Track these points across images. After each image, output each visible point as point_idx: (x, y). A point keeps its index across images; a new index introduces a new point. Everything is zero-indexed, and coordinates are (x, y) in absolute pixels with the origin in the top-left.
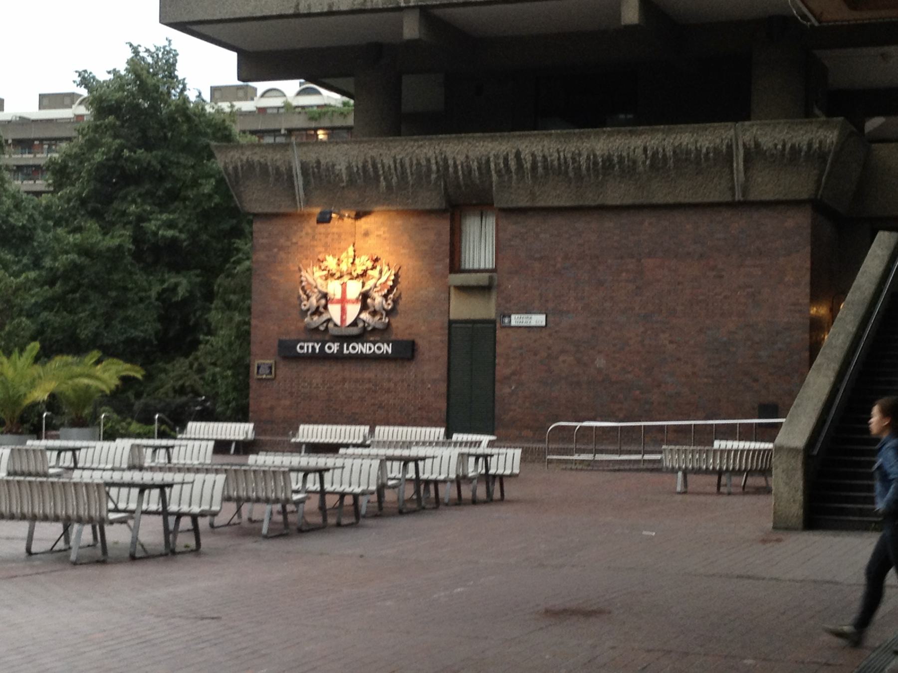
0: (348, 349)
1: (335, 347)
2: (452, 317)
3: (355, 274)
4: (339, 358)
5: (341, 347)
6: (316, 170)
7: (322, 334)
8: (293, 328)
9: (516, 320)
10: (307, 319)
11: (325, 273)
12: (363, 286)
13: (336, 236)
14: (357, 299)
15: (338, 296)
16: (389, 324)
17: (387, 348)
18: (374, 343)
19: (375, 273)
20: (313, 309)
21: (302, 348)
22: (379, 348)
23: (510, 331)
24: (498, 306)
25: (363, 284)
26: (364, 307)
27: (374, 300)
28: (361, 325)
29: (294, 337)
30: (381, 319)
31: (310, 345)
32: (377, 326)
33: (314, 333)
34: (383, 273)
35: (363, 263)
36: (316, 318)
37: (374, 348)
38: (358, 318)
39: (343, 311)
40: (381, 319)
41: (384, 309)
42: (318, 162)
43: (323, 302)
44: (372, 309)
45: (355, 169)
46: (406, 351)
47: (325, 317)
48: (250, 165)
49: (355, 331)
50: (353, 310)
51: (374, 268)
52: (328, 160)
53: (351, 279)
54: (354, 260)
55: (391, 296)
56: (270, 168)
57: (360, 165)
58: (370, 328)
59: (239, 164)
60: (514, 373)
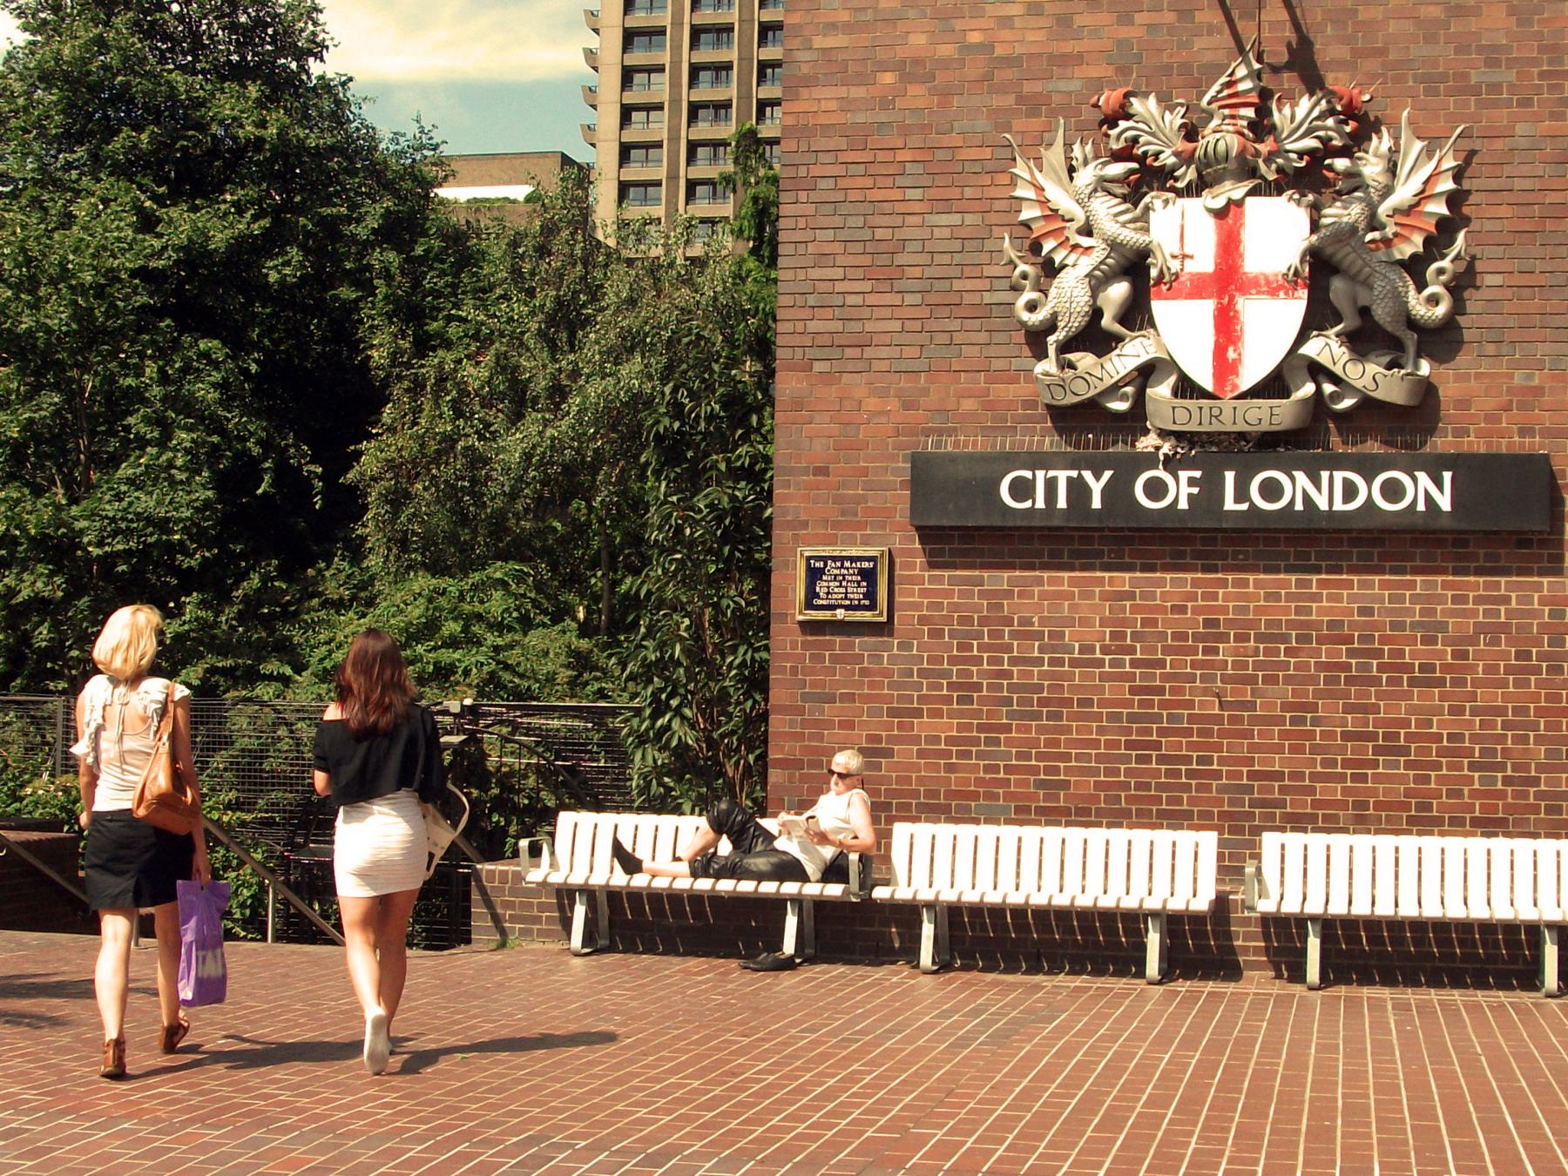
0: (1242, 494)
5: (1210, 489)
8: (968, 405)
11: (1118, 169)
12: (1315, 227)
14: (1291, 281)
15: (1204, 261)
20: (1077, 322)
21: (1022, 489)
29: (976, 443)
31: (1062, 476)
32: (1379, 395)
33: (1087, 424)
34: (1403, 172)
37: (1369, 491)
39: (1227, 327)
41: (1412, 323)
43: (1119, 291)
50: (1271, 328)
51: (1355, 144)
53: (1253, 192)
54: (1263, 111)
55: (1445, 263)
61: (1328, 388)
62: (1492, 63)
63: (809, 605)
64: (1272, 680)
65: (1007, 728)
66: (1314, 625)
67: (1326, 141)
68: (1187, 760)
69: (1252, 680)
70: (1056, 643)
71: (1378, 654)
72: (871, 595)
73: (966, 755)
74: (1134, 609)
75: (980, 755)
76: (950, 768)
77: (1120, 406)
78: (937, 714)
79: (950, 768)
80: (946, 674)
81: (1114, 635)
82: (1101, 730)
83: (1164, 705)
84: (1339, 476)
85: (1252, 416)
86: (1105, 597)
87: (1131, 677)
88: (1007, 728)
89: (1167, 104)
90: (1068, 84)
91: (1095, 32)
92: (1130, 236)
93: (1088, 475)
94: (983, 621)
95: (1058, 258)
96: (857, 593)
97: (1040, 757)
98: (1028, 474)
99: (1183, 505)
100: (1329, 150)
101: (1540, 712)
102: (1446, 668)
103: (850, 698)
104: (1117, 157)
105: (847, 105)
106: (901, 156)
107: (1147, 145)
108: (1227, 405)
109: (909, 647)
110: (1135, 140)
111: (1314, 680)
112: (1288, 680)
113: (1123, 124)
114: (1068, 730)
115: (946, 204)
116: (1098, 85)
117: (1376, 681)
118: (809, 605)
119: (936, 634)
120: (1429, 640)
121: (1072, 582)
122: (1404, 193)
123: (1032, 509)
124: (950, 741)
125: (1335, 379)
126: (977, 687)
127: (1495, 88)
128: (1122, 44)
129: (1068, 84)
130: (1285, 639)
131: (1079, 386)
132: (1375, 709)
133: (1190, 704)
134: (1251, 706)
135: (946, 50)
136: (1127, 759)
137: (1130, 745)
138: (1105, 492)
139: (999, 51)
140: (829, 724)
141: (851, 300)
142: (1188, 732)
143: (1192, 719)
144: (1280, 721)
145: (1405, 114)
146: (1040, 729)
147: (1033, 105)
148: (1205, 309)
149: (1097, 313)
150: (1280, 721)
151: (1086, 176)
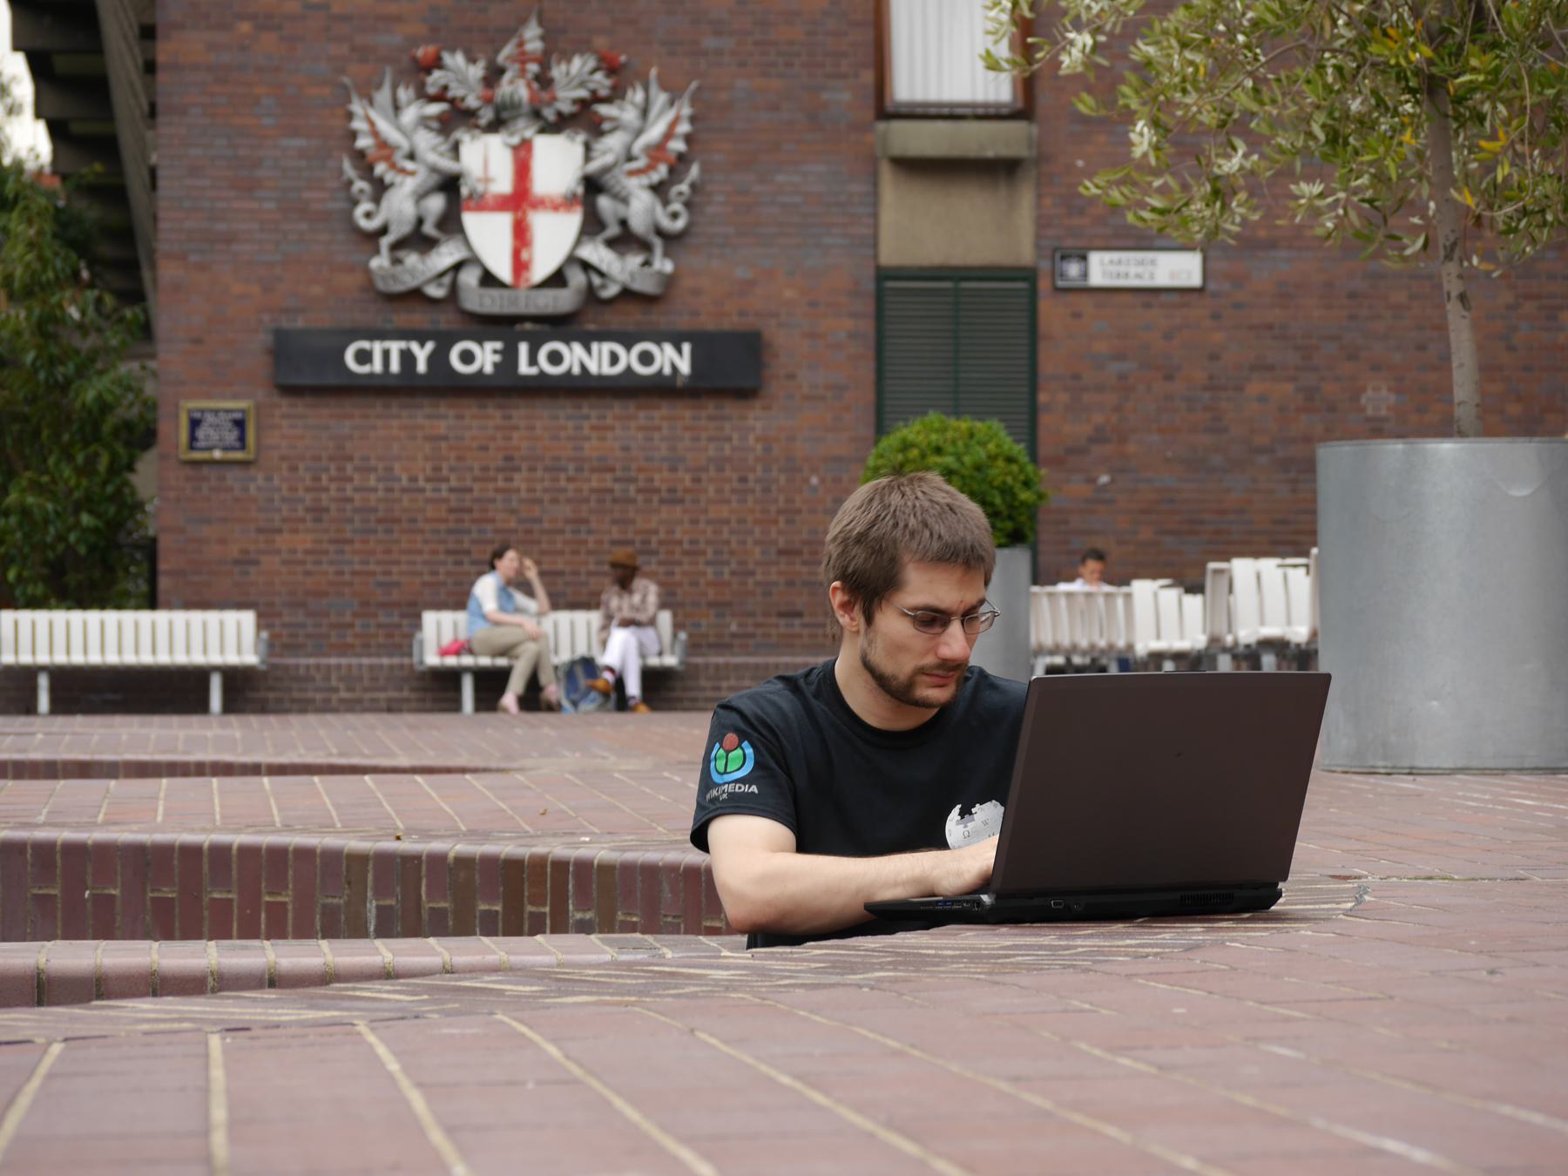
0: (533, 361)
1: (486, 357)
2: (890, 255)
3: (549, 114)
4: (506, 388)
5: (509, 356)
7: (445, 314)
8: (317, 290)
9: (1103, 268)
10: (380, 262)
11: (435, 109)
12: (588, 158)
14: (568, 202)
15: (503, 184)
16: (669, 281)
17: (673, 359)
18: (628, 342)
19: (627, 113)
21: (364, 357)
22: (646, 358)
23: (1085, 303)
24: (1042, 223)
25: (588, 148)
26: (592, 225)
27: (625, 201)
28: (577, 278)
30: (647, 263)
31: (395, 347)
35: (575, 75)
36: (411, 259)
37: (629, 359)
38: (572, 259)
39: (521, 234)
40: (647, 263)
41: (659, 232)
43: (436, 203)
44: (613, 230)
46: (733, 368)
47: (446, 256)
49: (561, 301)
50: (555, 238)
51: (616, 94)
53: (542, 131)
55: (684, 187)
58: (611, 291)
60: (1099, 437)
61: (597, 280)
62: (718, 33)
63: (192, 447)
64: (555, 501)
65: (351, 541)
69: (540, 501)
71: (634, 480)
72: (242, 438)
73: (318, 563)
74: (450, 448)
76: (308, 573)
77: (435, 291)
78: (295, 531)
79: (308, 573)
80: (302, 500)
81: (437, 469)
82: (426, 542)
87: (446, 500)
88: (351, 541)
89: (472, 60)
90: (392, 39)
92: (447, 164)
93: (414, 346)
95: (388, 178)
96: (231, 436)
99: (489, 369)
100: (596, 99)
101: (756, 522)
102: (686, 491)
104: (434, 99)
107: (455, 91)
108: (522, 293)
109: (269, 479)
110: (445, 88)
111: (587, 501)
112: (569, 501)
113: (437, 74)
114: (398, 542)
115: (295, 132)
116: (415, 42)
117: (633, 501)
118: (192, 447)
119: (294, 469)
120: (673, 469)
122: (655, 132)
123: (371, 375)
124: (307, 552)
125: (602, 274)
126: (327, 510)
127: (719, 52)
129: (392, 39)
132: (633, 522)
134: (539, 521)
137: (448, 552)
138: (431, 360)
139: (335, 10)
145: (653, 72)
149: (420, 221)
151: (410, 115)
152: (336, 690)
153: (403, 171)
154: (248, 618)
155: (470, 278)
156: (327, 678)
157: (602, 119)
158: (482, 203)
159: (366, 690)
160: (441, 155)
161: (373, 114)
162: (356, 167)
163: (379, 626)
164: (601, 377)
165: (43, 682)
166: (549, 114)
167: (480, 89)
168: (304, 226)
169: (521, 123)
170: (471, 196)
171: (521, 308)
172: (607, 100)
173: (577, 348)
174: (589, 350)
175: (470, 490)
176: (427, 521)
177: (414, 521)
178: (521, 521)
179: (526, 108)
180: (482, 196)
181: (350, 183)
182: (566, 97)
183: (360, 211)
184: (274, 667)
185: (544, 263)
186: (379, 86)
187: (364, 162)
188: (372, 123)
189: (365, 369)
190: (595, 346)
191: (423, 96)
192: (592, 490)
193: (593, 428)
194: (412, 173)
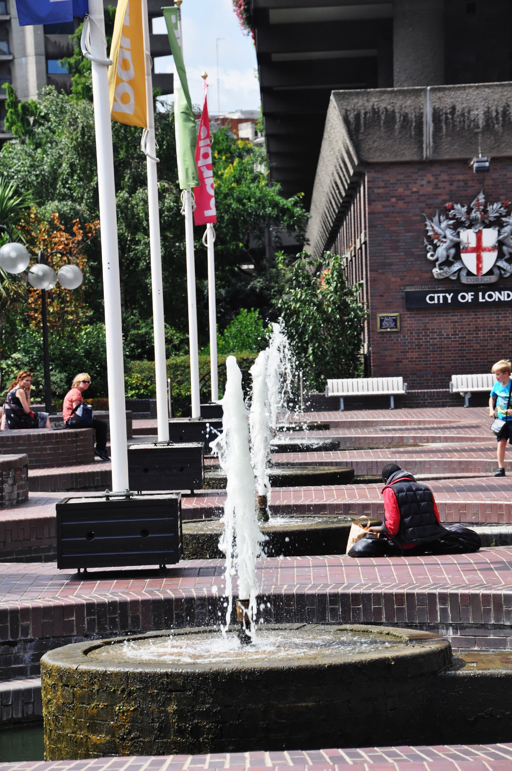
0: (483, 298)
1: (469, 297)
5: (476, 297)
6: (450, 116)
8: (417, 279)
10: (436, 271)
11: (451, 222)
12: (499, 235)
13: (462, 184)
15: (473, 244)
20: (444, 259)
21: (432, 299)
25: (499, 231)
28: (496, 271)
31: (441, 295)
36: (446, 268)
38: (495, 266)
39: (479, 260)
42: (454, 108)
43: (452, 251)
45: (494, 114)
48: (375, 112)
49: (493, 279)
50: (489, 259)
52: (464, 105)
53: (484, 228)
54: (486, 206)
56: (398, 115)
57: (500, 109)
59: (363, 112)
61: (503, 272)
63: (381, 328)
64: (491, 340)
65: (429, 354)
66: (501, 327)
67: (501, 214)
68: (472, 359)
69: (487, 340)
70: (440, 334)
72: (396, 325)
73: (420, 361)
75: (423, 361)
77: (454, 278)
78: (413, 352)
79: (416, 364)
80: (414, 343)
81: (454, 331)
82: (452, 354)
83: (467, 347)
84: (506, 292)
85: (486, 280)
86: (452, 322)
87: (458, 341)
88: (429, 354)
89: (463, 206)
90: (439, 200)
91: (444, 188)
92: (456, 239)
93: (447, 295)
94: (423, 330)
95: (438, 244)
96: (392, 325)
97: (438, 360)
98: (433, 295)
99: (470, 301)
100: (501, 216)
103: (392, 349)
105: (384, 207)
106: (398, 219)
107: (458, 216)
108: (480, 277)
110: (455, 215)
111: (501, 339)
112: (496, 339)
113: (452, 211)
114: (444, 354)
115: (409, 231)
116: (445, 201)
118: (381, 328)
119: (411, 333)
121: (444, 319)
124: (416, 358)
125: (504, 270)
126: (422, 345)
128: (451, 191)
130: (494, 330)
131: (444, 274)
133: (472, 346)
134: (487, 346)
135: (408, 193)
136: (458, 360)
137: (459, 357)
138: (452, 298)
139: (421, 193)
140: (386, 356)
141: (387, 254)
142: (472, 353)
143: (473, 350)
144: (494, 349)
146: (438, 354)
147: (429, 206)
148: (474, 255)
150: (494, 349)
151: (443, 225)
152: (427, 400)
153: (442, 242)
154: (400, 379)
155: (464, 273)
156: (424, 396)
157: (504, 222)
158: (467, 250)
159: (436, 399)
160: (454, 236)
161: (433, 225)
162: (428, 241)
163: (439, 379)
164: (504, 301)
165: (342, 400)
166: (487, 221)
167: (465, 216)
168: (413, 260)
169: (478, 225)
170: (463, 248)
171: (480, 282)
172: (505, 216)
173: (497, 293)
174: (501, 294)
175: (465, 337)
176: (452, 347)
177: (448, 347)
178: (481, 346)
179: (480, 221)
180: (467, 248)
181: (426, 246)
182: (492, 215)
183: (429, 255)
184: (408, 393)
185: (487, 267)
186: (434, 216)
187: (430, 240)
188: (433, 227)
189: (433, 302)
190: (503, 292)
191: (448, 218)
192: (503, 336)
193: (503, 317)
194: (445, 242)
